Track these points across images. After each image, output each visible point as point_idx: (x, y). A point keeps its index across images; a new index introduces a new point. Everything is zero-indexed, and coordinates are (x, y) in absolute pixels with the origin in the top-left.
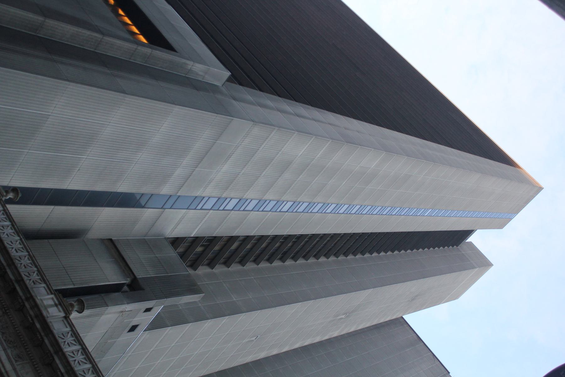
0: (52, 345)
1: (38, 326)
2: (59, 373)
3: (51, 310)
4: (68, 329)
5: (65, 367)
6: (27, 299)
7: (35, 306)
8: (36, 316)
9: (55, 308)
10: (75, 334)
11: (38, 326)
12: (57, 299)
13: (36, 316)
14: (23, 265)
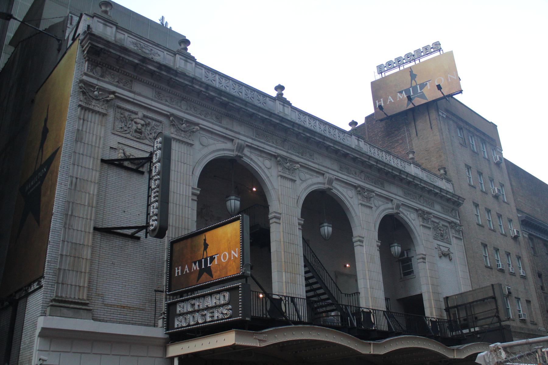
1: (308, 135)
5: (331, 143)
11: (308, 135)
13: (304, 131)
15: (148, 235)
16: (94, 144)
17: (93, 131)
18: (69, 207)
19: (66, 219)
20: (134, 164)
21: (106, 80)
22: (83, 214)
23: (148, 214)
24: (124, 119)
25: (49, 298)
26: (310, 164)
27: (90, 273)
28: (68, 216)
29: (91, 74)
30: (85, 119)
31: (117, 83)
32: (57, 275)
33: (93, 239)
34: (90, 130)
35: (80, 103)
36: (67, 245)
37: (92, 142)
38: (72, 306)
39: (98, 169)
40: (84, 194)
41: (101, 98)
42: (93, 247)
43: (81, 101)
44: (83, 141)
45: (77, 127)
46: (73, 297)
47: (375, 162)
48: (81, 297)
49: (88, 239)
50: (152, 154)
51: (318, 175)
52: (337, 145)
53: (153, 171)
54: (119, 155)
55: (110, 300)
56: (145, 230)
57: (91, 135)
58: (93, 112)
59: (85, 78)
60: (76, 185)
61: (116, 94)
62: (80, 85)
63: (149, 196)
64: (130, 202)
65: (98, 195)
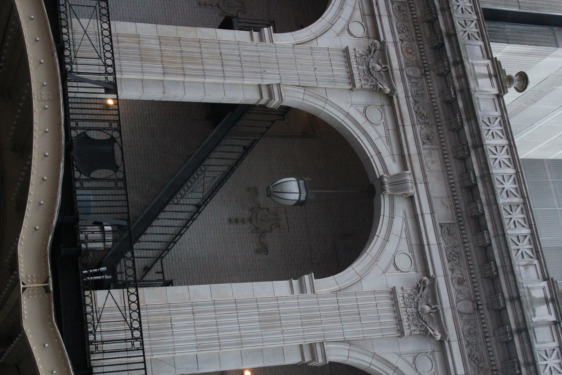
0: (472, 136)
1: (461, 104)
2: (472, 175)
3: (481, 81)
4: (498, 113)
5: (481, 170)
6: (456, 64)
7: (463, 76)
8: (461, 91)
9: (488, 80)
10: (504, 122)
11: (461, 104)
12: (494, 68)
13: (461, 91)
14: (460, 8)
26: (408, 122)
47: (517, 323)
51: (396, 157)
52: (484, 186)
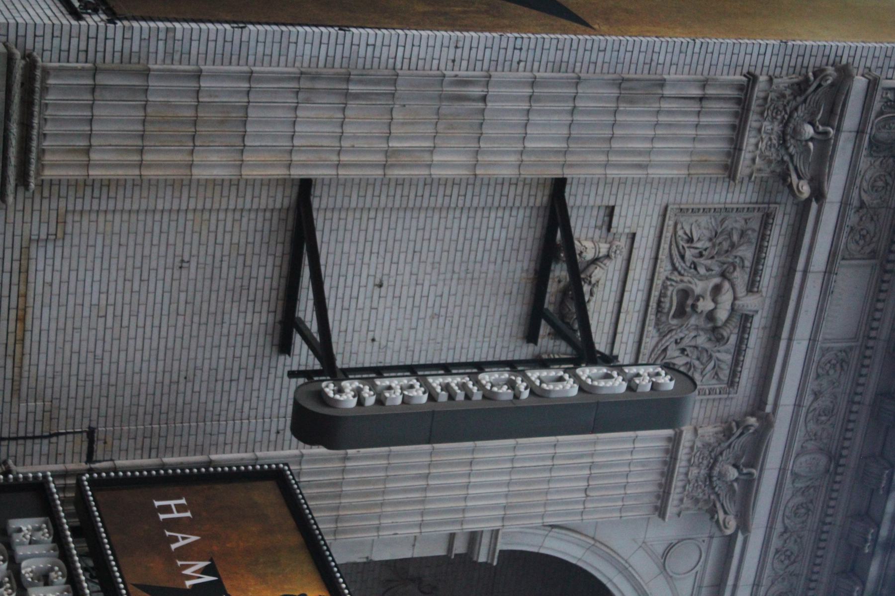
15: (301, 381)
16: (616, 145)
17: (664, 139)
18: (378, 82)
19: (330, 79)
20: (562, 304)
21: (864, 163)
22: (355, 137)
23: (380, 371)
24: (723, 243)
25: (38, 46)
27: (139, 183)
28: (343, 84)
29: (877, 105)
30: (706, 104)
31: (856, 203)
32: (129, 67)
33: (267, 183)
34: (670, 125)
35: (763, 78)
36: (238, 92)
37: (624, 138)
38: (14, 129)
39: (528, 173)
40: (430, 130)
41: (792, 150)
42: (236, 184)
43: (771, 80)
44: (622, 107)
45: (673, 76)
46: (49, 128)
48: (48, 158)
49: (265, 165)
50: (609, 360)
53: (544, 373)
54: (587, 245)
55: (45, 268)
56: (318, 366)
57: (650, 133)
58: (733, 127)
59: (859, 84)
60: (459, 98)
61: (814, 206)
62: (830, 70)
63: (447, 368)
64: (415, 298)
65: (429, 182)
